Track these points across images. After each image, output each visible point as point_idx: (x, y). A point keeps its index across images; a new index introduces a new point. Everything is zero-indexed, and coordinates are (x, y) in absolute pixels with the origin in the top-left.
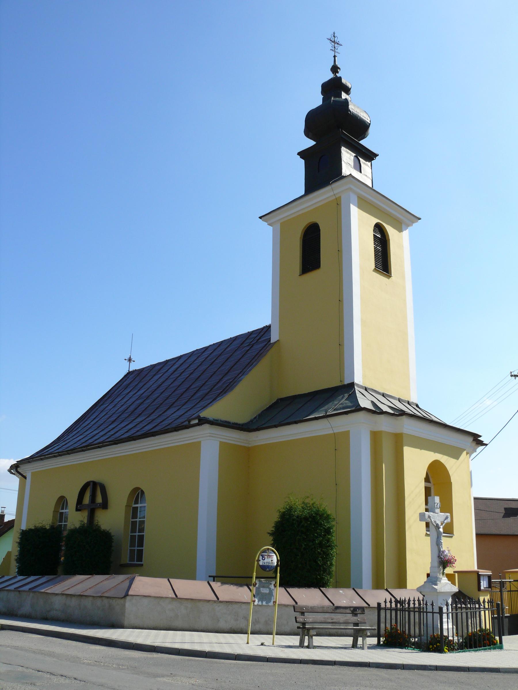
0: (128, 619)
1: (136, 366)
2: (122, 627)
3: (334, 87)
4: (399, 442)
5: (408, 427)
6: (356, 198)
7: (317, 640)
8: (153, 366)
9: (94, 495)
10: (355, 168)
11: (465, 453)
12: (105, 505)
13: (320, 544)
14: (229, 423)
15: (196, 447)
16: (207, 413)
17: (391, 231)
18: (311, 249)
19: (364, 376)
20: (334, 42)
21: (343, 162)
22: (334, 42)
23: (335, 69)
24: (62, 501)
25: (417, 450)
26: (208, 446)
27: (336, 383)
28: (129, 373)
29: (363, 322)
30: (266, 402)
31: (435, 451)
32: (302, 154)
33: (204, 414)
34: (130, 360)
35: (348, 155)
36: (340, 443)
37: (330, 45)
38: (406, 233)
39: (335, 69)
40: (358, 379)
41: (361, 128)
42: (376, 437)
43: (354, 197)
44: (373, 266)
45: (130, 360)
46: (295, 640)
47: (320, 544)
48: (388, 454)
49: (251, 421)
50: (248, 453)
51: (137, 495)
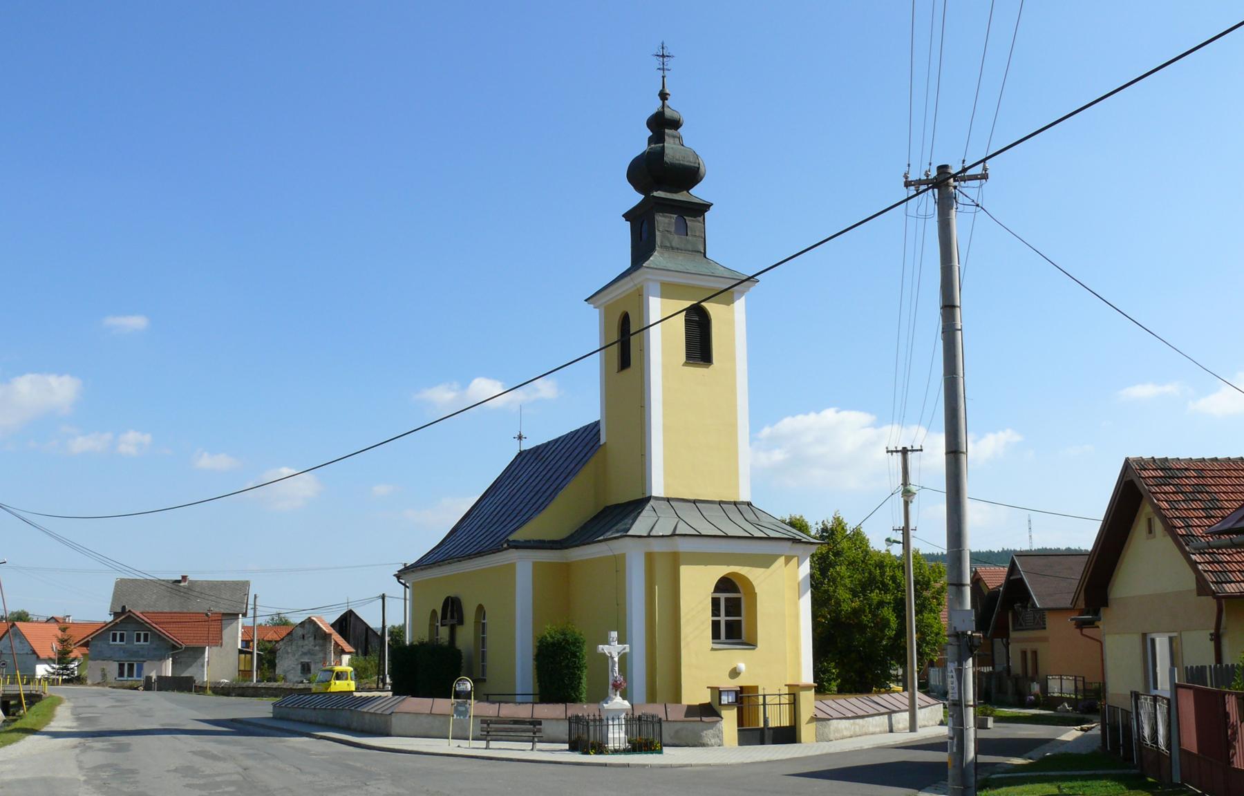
0: (394, 730)
1: (527, 445)
2: (388, 735)
3: (662, 124)
4: (675, 560)
5: (683, 546)
6: (658, 286)
7: (493, 744)
8: (538, 447)
9: (452, 609)
10: (677, 232)
11: (782, 560)
12: (461, 622)
13: (567, 666)
14: (543, 541)
15: (511, 568)
16: (520, 535)
17: (711, 307)
18: (625, 344)
19: (666, 486)
20: (663, 56)
21: (657, 233)
22: (663, 56)
23: (663, 96)
24: (434, 612)
25: (703, 567)
26: (523, 565)
27: (640, 497)
28: (521, 453)
29: (666, 429)
30: (591, 512)
31: (728, 564)
32: (627, 216)
33: (511, 538)
34: (520, 438)
35: (666, 220)
36: (618, 565)
37: (657, 62)
38: (740, 305)
39: (663, 96)
40: (658, 489)
41: (690, 175)
42: (650, 557)
43: (657, 287)
44: (684, 359)
45: (520, 438)
46: (483, 744)
47: (567, 666)
48: (664, 572)
49: (572, 535)
50: (566, 568)
51: (480, 609)
